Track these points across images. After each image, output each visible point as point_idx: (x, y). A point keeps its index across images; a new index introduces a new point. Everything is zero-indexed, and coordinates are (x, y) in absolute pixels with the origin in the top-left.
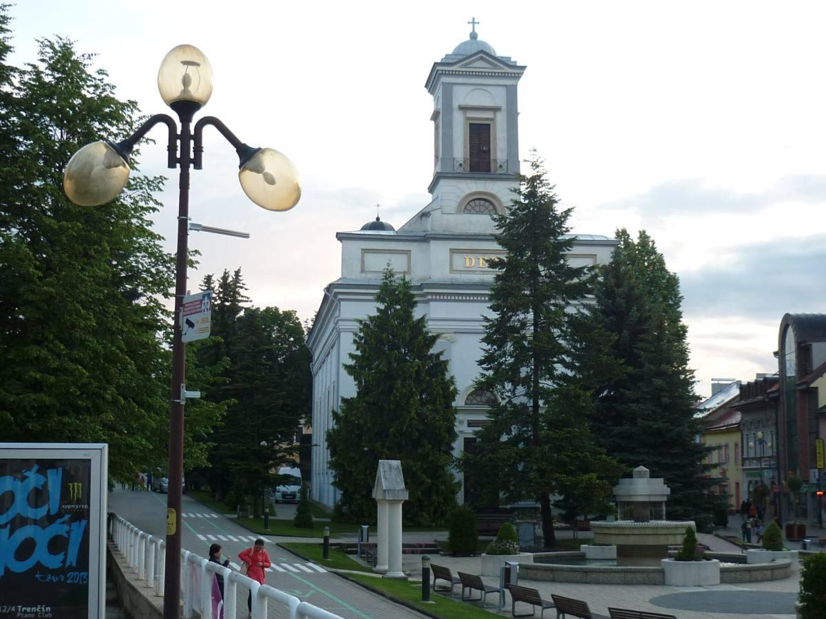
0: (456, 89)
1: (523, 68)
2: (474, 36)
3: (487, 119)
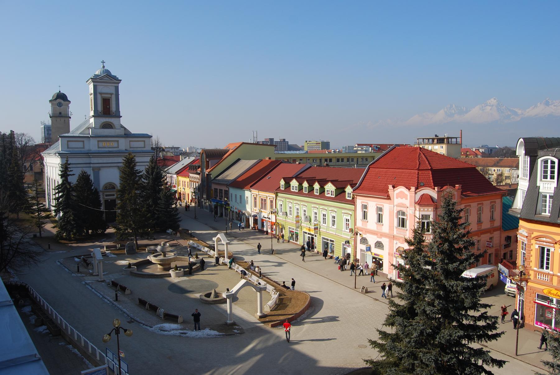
1: (121, 80)
2: (104, 67)
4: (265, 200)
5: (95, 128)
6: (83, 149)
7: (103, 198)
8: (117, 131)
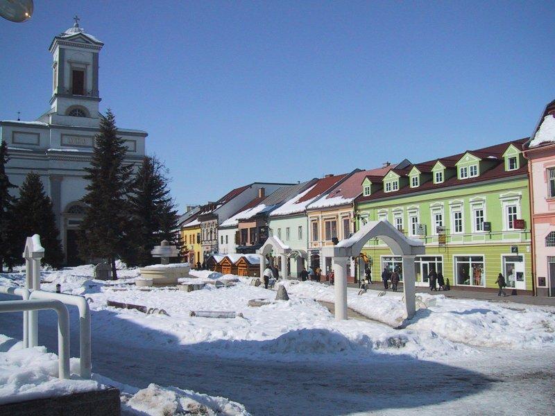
4: (334, 223)
5: (57, 114)
6: (36, 147)
7: (65, 225)
8: (92, 120)
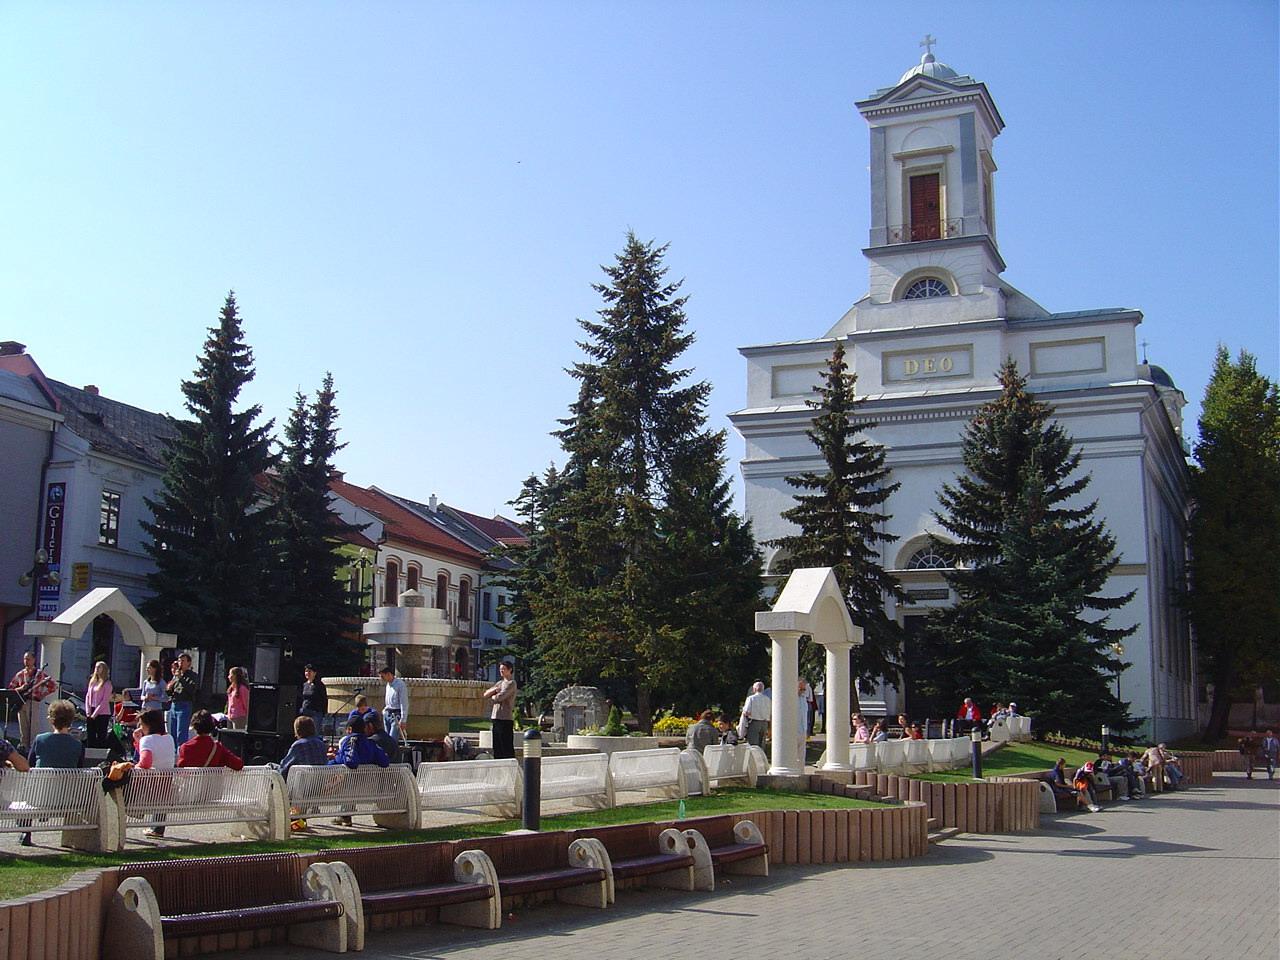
0: (892, 134)
3: (933, 167)
